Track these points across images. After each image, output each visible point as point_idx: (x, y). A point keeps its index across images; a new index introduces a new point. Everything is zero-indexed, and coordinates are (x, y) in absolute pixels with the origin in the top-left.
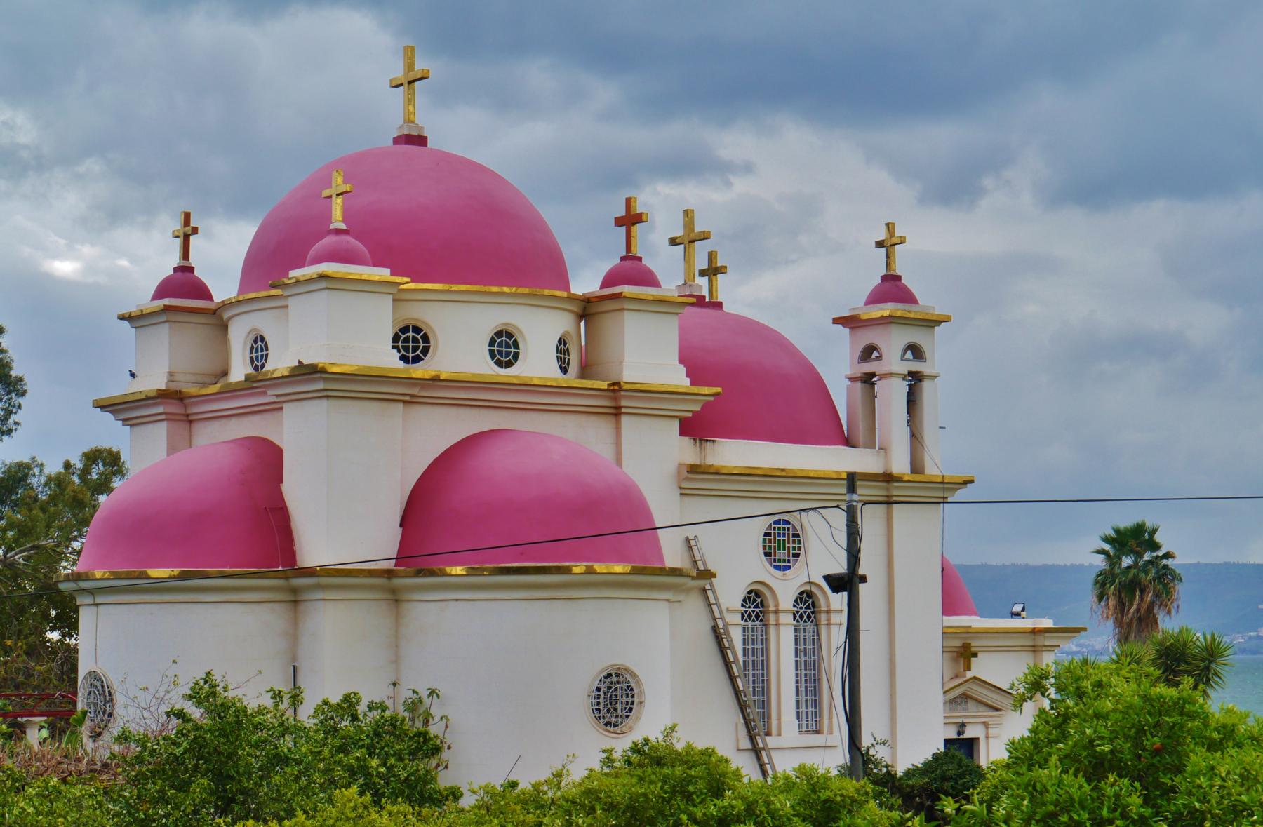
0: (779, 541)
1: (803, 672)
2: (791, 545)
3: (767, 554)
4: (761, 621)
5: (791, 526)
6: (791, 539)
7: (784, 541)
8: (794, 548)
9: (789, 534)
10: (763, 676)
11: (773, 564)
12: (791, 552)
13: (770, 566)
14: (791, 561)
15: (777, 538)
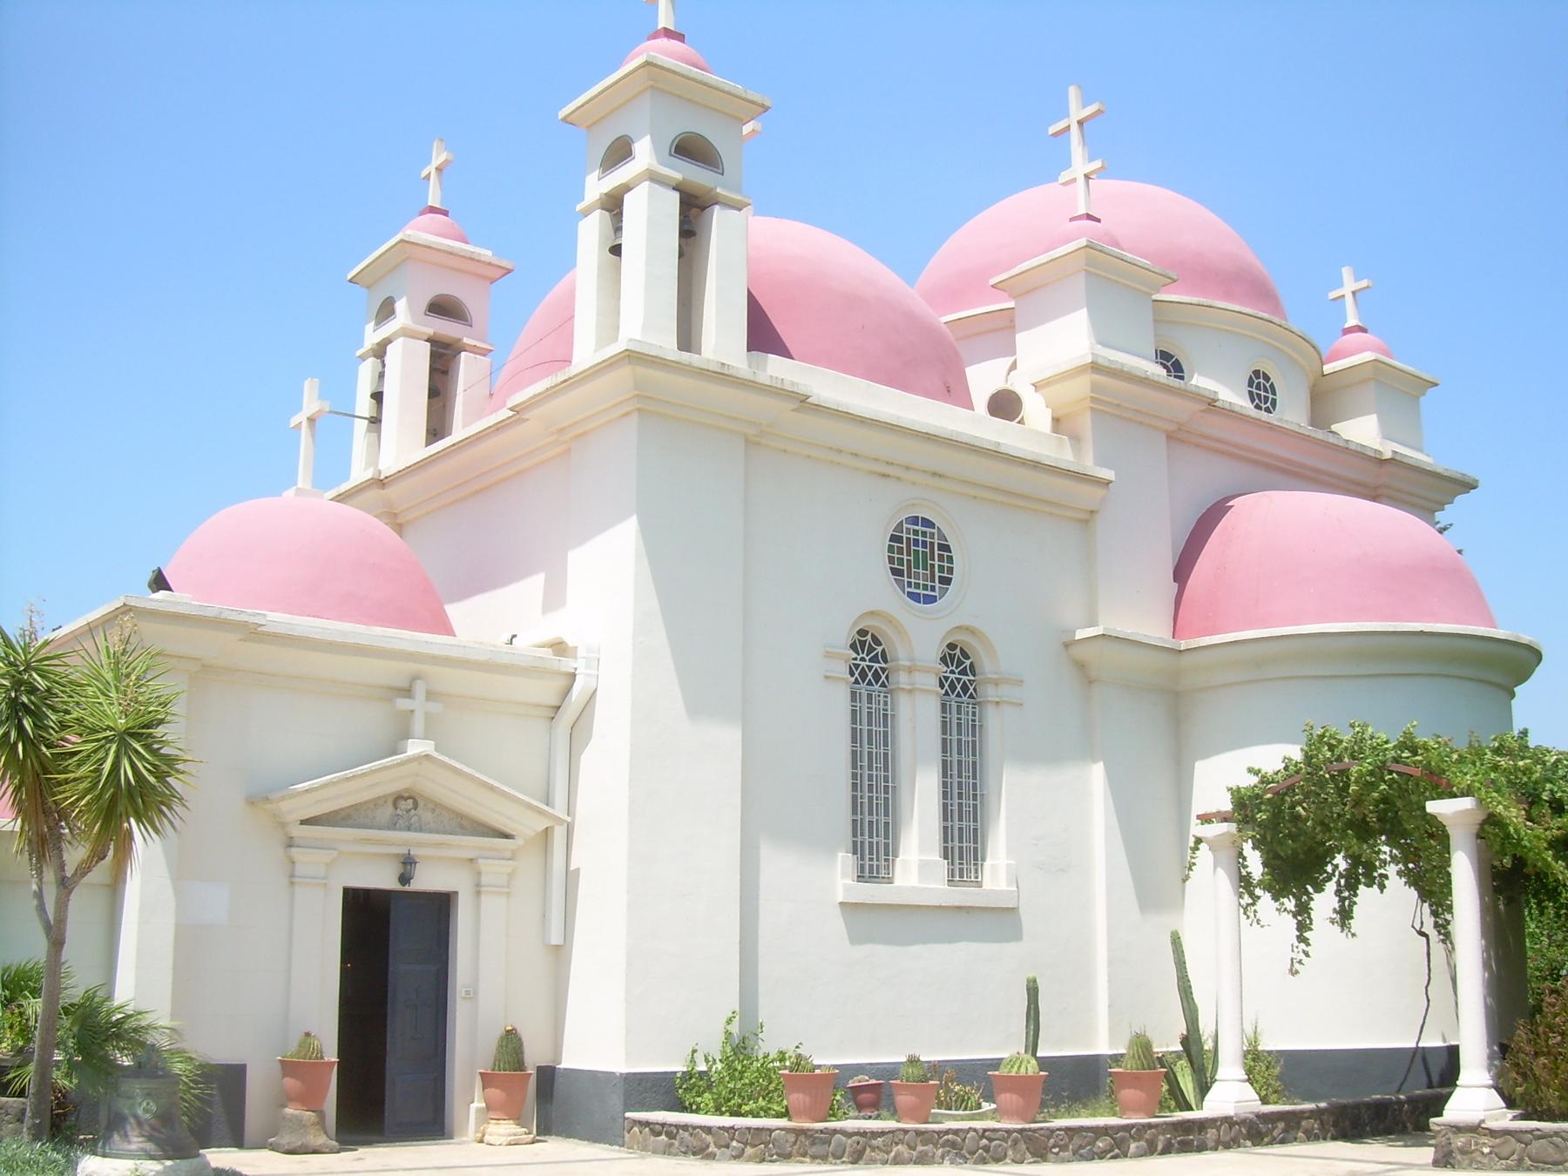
0: (917, 552)
1: (956, 779)
2: (936, 563)
3: (895, 572)
5: (935, 531)
6: (936, 552)
8: (941, 569)
9: (932, 544)
10: (886, 781)
11: (907, 590)
12: (937, 574)
13: (901, 593)
14: (937, 589)
15: (912, 548)
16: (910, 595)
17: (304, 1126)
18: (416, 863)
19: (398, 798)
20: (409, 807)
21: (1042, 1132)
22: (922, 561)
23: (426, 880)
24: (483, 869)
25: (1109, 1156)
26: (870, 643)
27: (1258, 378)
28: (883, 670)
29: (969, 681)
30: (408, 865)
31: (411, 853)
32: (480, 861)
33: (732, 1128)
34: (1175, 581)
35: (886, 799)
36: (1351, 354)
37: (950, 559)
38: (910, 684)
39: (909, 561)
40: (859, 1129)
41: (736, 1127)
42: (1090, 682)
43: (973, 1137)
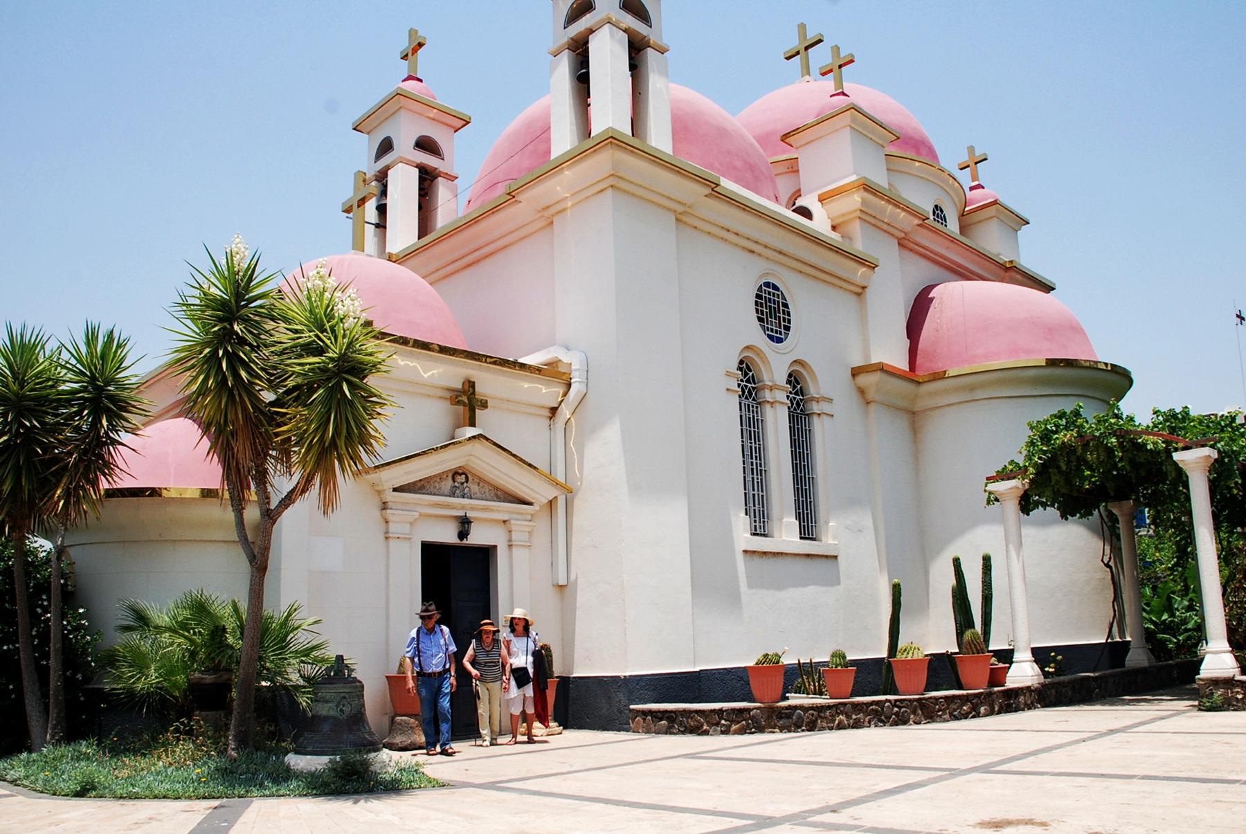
0: (770, 306)
2: (782, 315)
3: (760, 320)
4: (754, 400)
5: (780, 293)
6: (781, 308)
7: (775, 308)
8: (784, 318)
9: (778, 302)
11: (767, 332)
12: (782, 323)
16: (769, 336)
17: (411, 727)
18: (471, 522)
19: (455, 474)
20: (463, 481)
21: (931, 700)
22: (773, 313)
23: (477, 537)
24: (514, 528)
25: (970, 716)
26: (745, 370)
27: (937, 210)
28: (754, 388)
29: (800, 399)
30: (464, 525)
31: (468, 515)
32: (512, 522)
33: (721, 710)
34: (908, 338)
35: (761, 479)
36: (980, 202)
37: (789, 314)
38: (772, 398)
39: (779, 313)
40: (813, 704)
41: (724, 709)
42: (868, 403)
43: (888, 706)
